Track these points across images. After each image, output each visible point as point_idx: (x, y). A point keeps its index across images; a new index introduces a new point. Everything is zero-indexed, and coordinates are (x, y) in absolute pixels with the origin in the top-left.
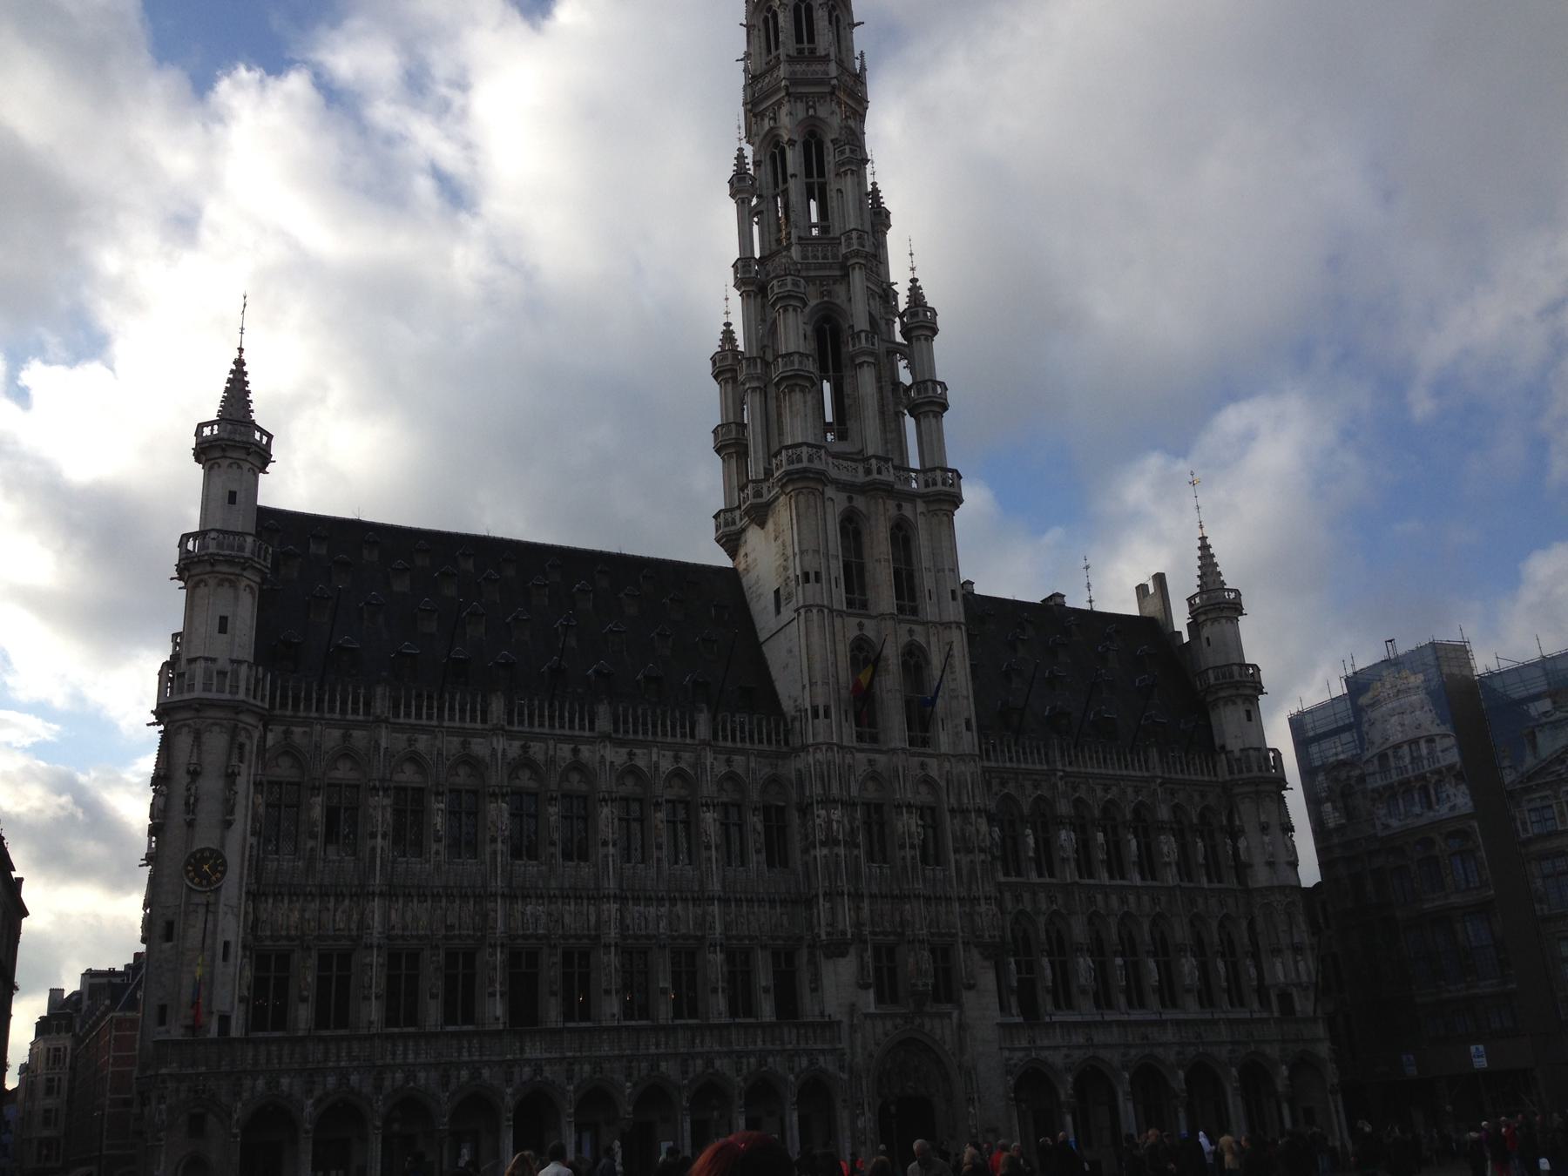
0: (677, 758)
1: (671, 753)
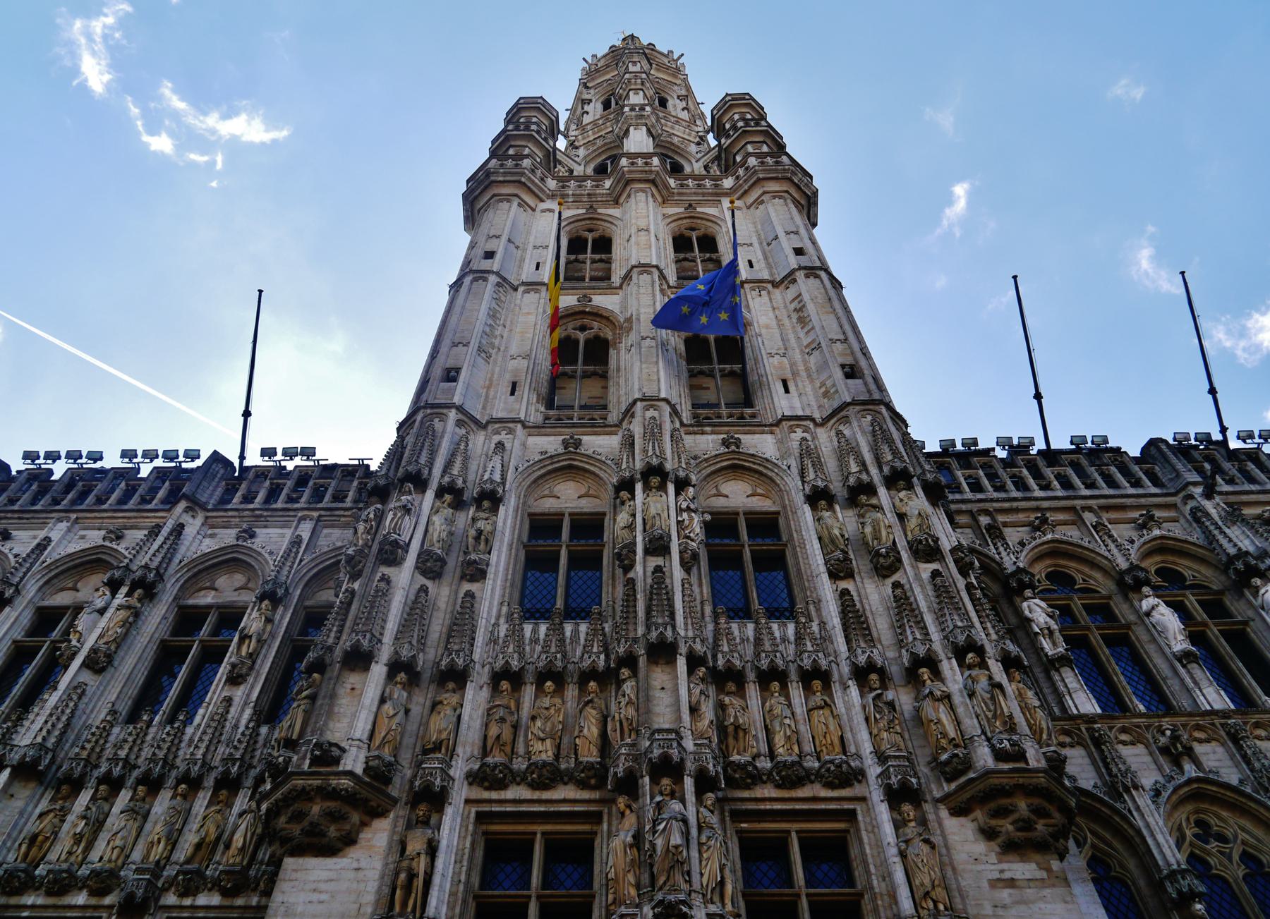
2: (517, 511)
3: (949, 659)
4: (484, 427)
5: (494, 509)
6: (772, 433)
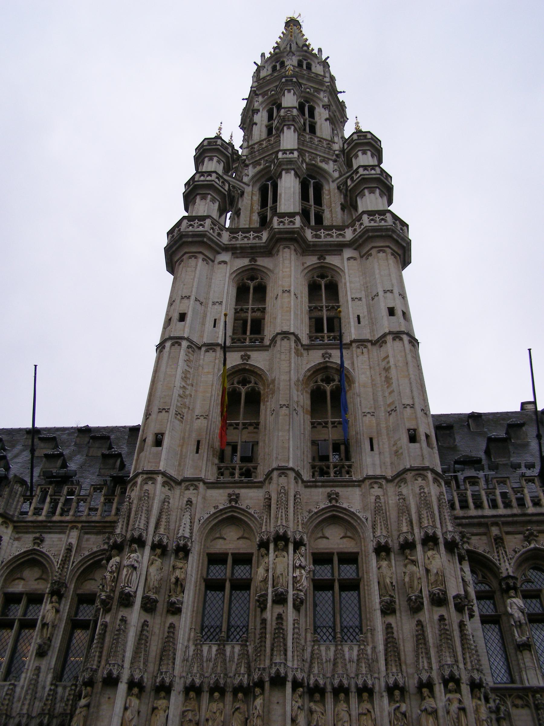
2: (200, 555)
3: (440, 683)
4: (179, 483)
6: (359, 486)
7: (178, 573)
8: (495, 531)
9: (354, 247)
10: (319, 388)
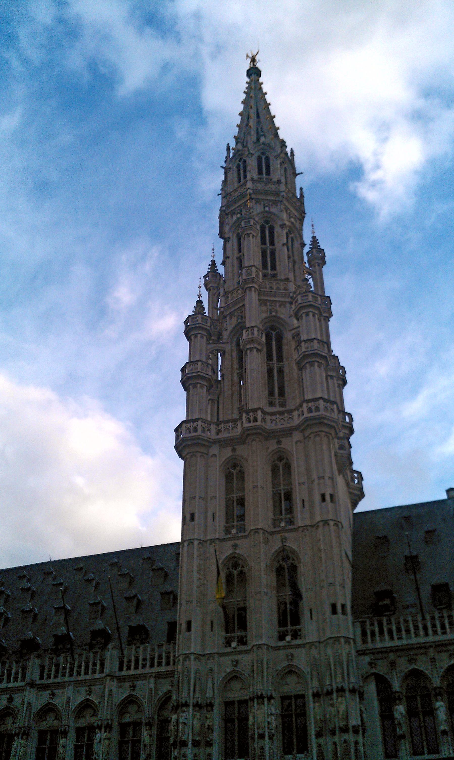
0: (90, 692)
1: (84, 689)
5: (212, 710)
6: (304, 647)
7: (208, 722)
8: (392, 656)
9: (300, 429)
10: (280, 566)
